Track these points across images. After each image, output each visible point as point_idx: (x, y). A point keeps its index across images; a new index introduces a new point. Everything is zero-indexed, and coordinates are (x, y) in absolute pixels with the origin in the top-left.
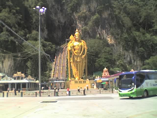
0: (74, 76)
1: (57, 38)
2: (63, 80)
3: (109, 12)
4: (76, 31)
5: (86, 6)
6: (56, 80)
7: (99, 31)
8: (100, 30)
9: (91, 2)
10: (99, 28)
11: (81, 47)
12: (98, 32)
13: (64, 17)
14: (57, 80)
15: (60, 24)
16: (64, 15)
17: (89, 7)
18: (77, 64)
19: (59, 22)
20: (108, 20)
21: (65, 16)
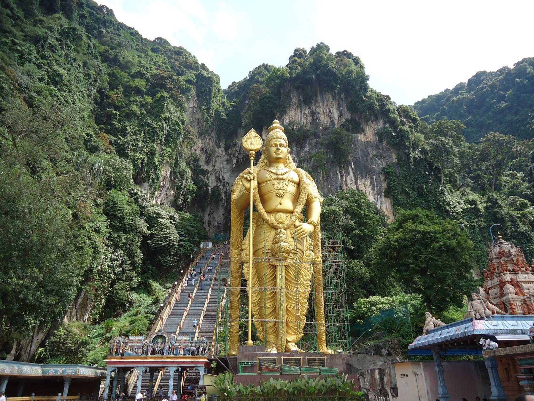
0: (260, 336)
1: (209, 224)
2: (193, 353)
3: (377, 124)
4: (274, 125)
5: (301, 111)
6: (150, 350)
7: (349, 182)
8: (351, 179)
9: (319, 98)
10: (348, 173)
11: (296, 186)
12: (346, 185)
13: (234, 166)
14: (153, 353)
15: (221, 187)
16: (234, 162)
17: (313, 113)
18: (275, 267)
19: (218, 179)
20: (377, 148)
21: (237, 162)
